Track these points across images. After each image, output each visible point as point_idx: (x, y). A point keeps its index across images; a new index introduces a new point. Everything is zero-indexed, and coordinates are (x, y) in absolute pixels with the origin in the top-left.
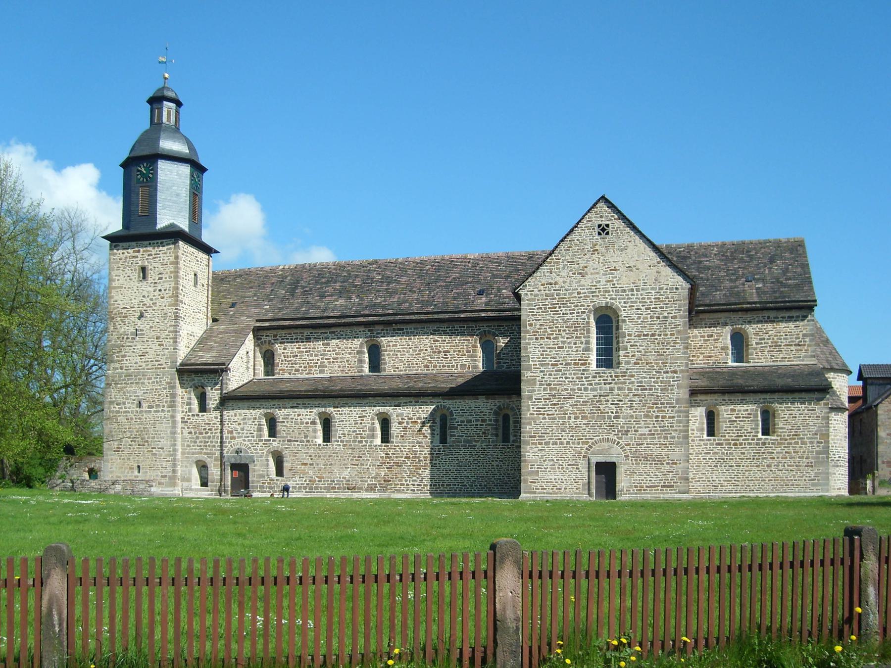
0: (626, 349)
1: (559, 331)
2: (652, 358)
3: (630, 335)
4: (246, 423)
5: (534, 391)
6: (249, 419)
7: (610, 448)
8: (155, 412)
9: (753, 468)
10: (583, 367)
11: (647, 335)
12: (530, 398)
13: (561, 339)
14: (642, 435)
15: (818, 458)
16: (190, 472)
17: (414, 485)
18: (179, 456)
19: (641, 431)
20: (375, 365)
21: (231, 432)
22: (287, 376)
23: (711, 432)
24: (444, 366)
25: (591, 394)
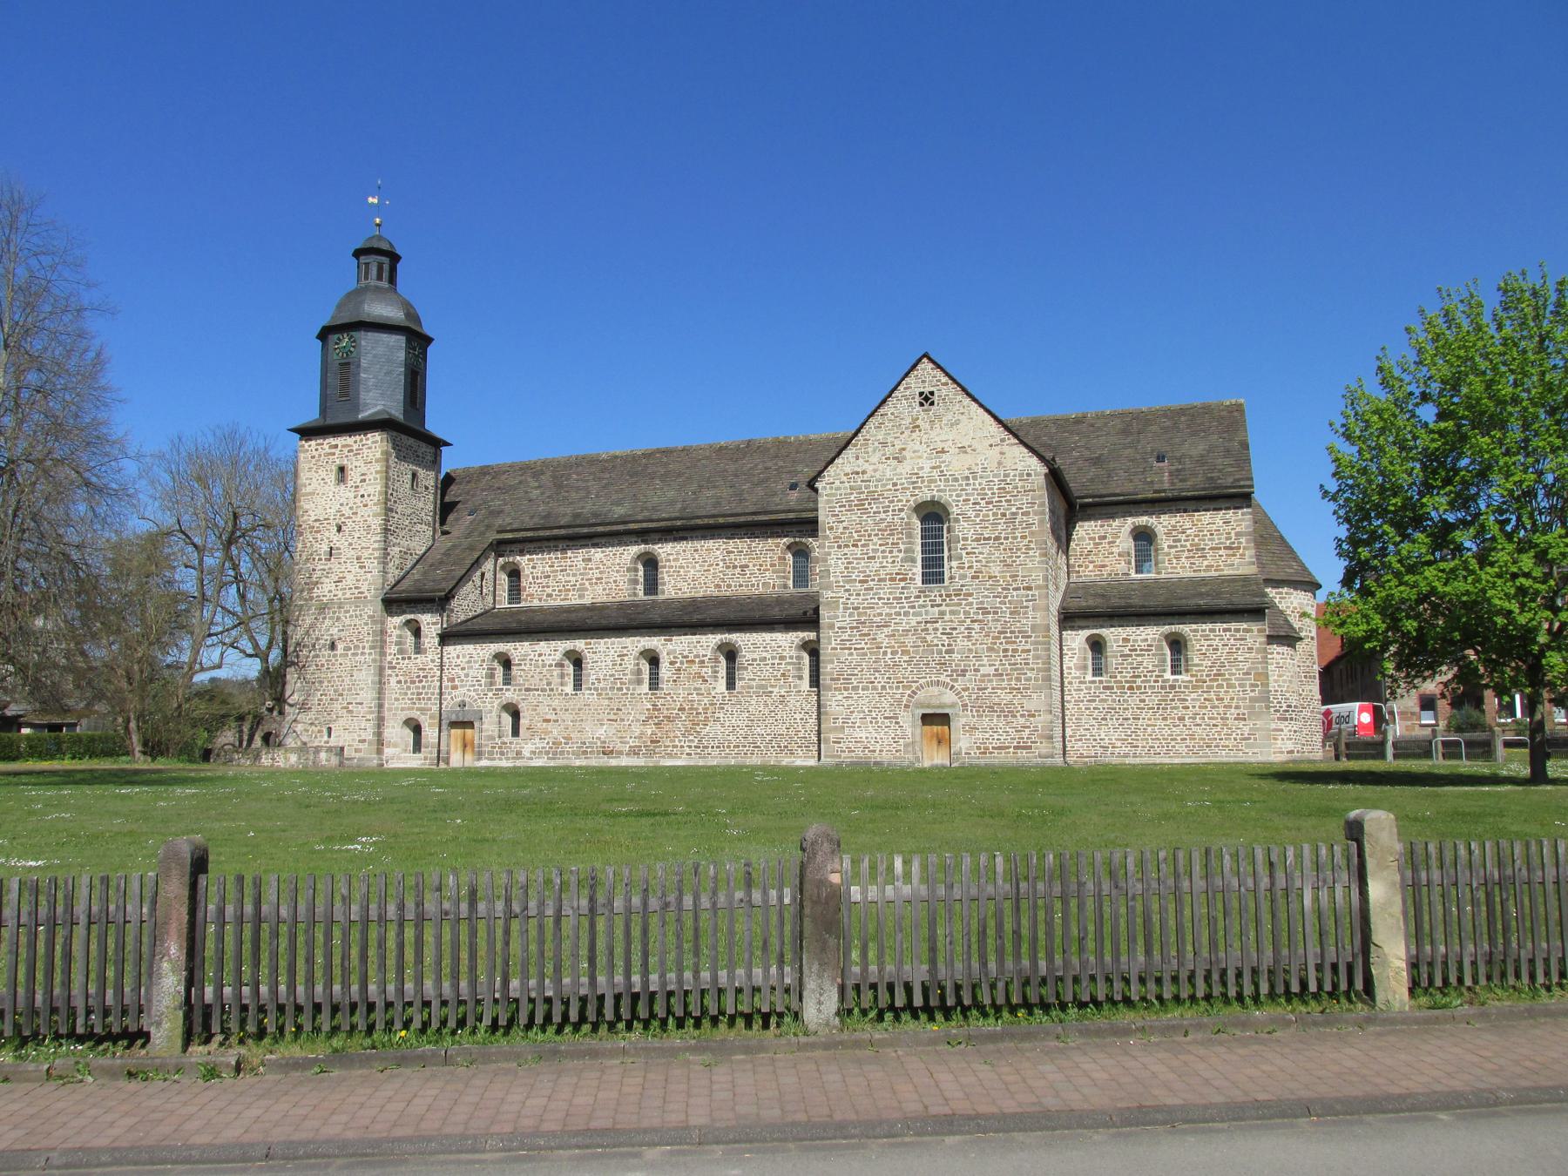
2: (995, 570)
19: (983, 670)
21: (452, 680)
22: (536, 603)
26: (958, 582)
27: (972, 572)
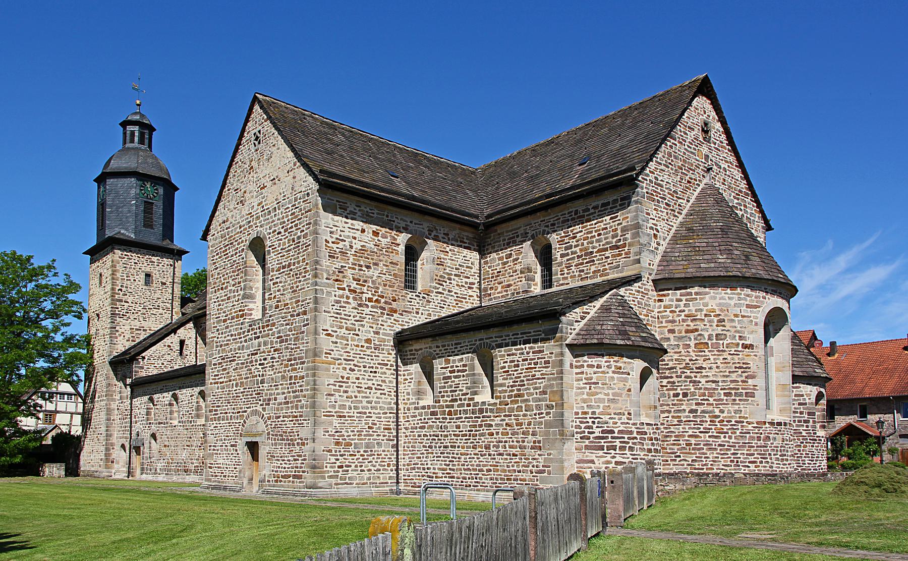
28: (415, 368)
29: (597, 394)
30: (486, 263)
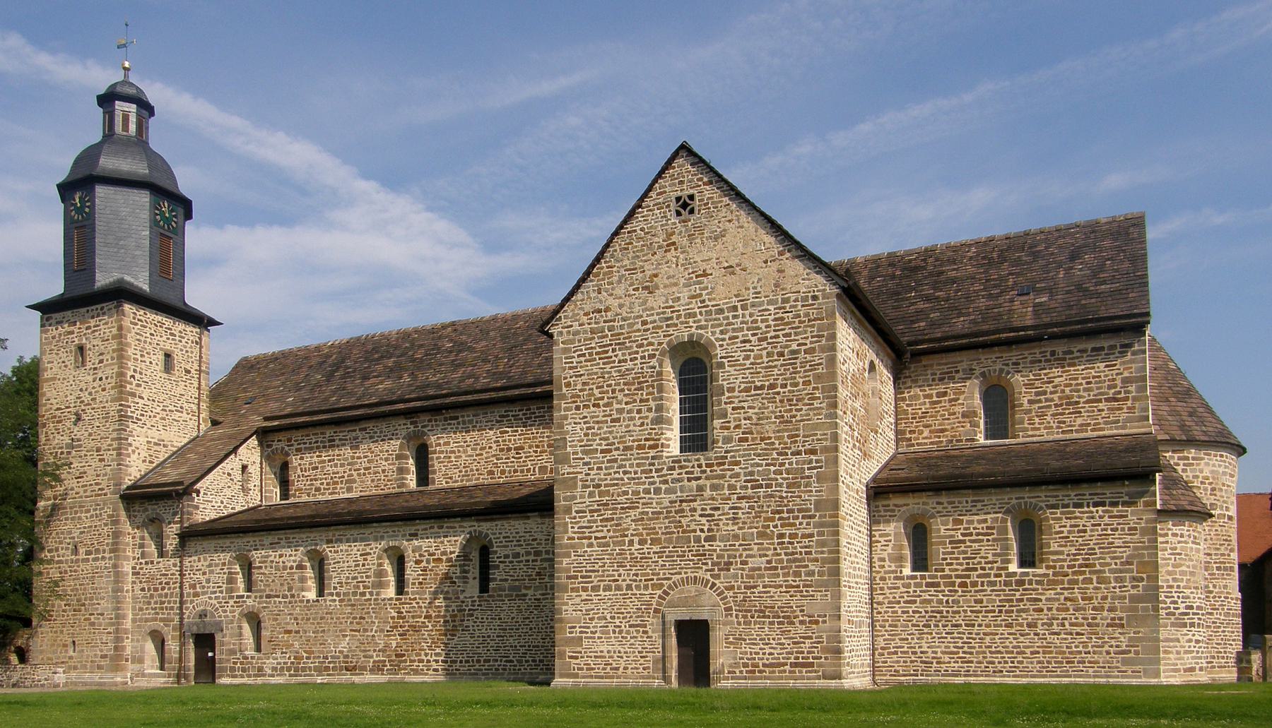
0: (725, 416)
1: (614, 391)
2: (770, 428)
3: (731, 390)
4: (211, 572)
5: (574, 498)
6: (217, 565)
7: (701, 594)
8: (94, 560)
9: (1000, 630)
10: (652, 453)
11: (762, 388)
12: (568, 510)
13: (616, 406)
14: (753, 569)
15: (1136, 609)
16: (143, 651)
17: (437, 661)
18: (128, 624)
19: (753, 563)
20: (424, 476)
21: (193, 586)
22: (305, 498)
23: (920, 562)
24: (515, 471)
25: (666, 499)
26: (721, 447)
27: (737, 435)
28: (894, 530)
29: (1181, 565)
30: (904, 399)
